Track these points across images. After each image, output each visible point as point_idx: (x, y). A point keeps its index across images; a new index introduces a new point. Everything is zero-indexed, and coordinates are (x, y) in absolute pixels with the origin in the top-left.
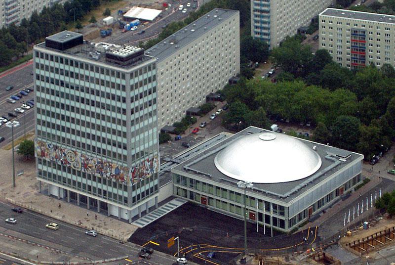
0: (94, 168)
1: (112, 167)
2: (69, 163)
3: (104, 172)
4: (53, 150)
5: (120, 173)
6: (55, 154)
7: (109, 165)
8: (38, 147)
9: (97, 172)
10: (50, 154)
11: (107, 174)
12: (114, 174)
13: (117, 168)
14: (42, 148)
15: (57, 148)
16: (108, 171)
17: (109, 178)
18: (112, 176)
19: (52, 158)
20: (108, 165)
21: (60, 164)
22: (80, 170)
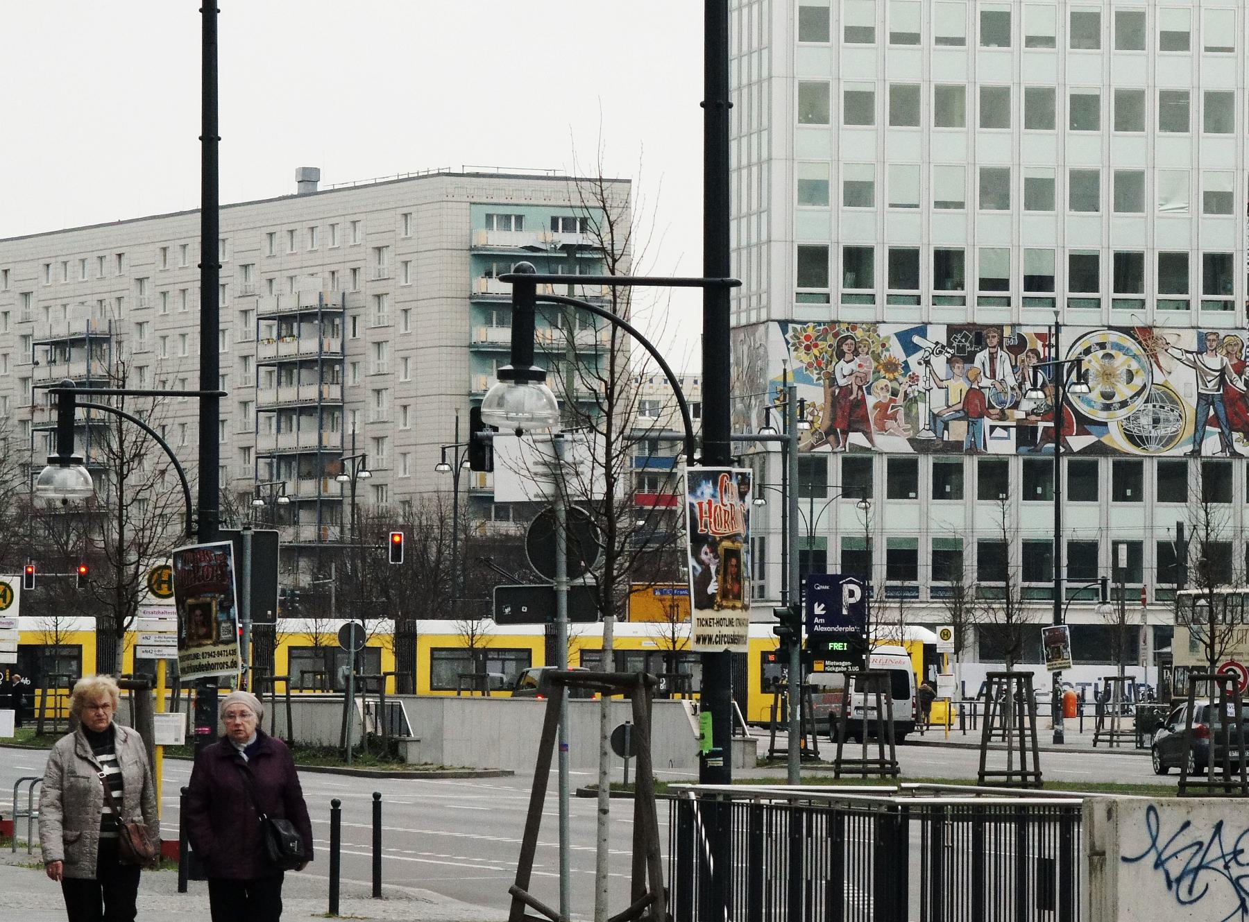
2: (1085, 424)
4: (939, 362)
6: (959, 387)
10: (911, 401)
14: (844, 370)
19: (934, 417)
21: (1002, 445)
22: (1179, 451)
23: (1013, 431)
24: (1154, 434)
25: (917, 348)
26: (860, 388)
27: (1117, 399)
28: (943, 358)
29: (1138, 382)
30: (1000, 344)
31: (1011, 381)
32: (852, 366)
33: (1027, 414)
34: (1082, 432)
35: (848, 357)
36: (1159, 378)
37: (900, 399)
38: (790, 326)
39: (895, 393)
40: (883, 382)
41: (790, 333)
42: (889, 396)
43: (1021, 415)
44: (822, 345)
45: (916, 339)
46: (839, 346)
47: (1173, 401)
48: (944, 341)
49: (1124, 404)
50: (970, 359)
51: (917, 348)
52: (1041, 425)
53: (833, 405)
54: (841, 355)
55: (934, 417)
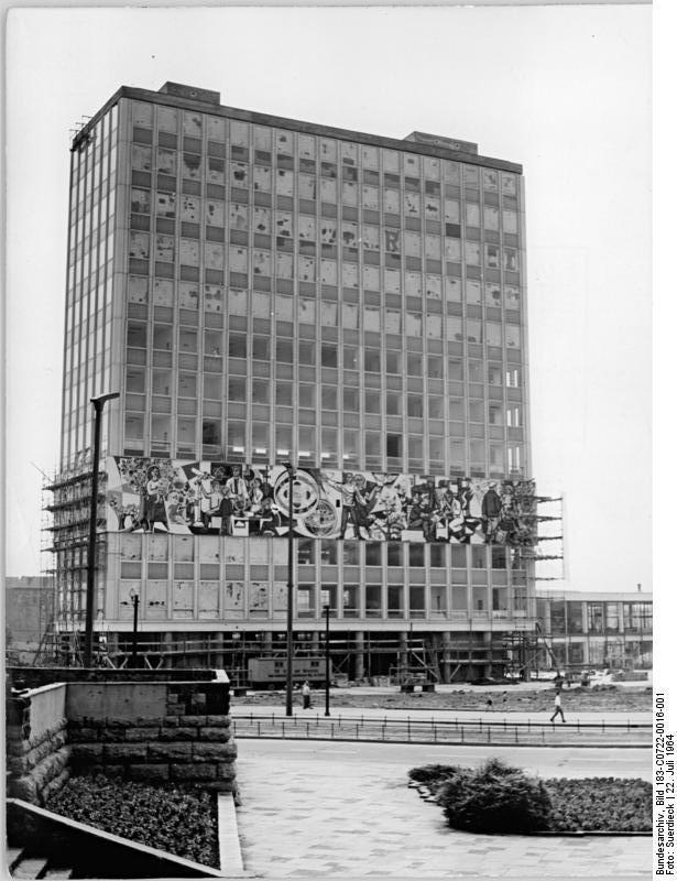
0: (399, 512)
1: (469, 498)
3: (438, 518)
4: (207, 484)
5: (502, 506)
6: (217, 498)
7: (461, 489)
8: (125, 488)
9: (410, 528)
10: (190, 505)
11: (452, 525)
12: (480, 515)
13: (492, 492)
14: (151, 485)
15: (229, 472)
16: (457, 512)
17: (457, 536)
18: (473, 526)
19: (203, 514)
20: (454, 489)
23: (247, 523)
24: (321, 526)
25: (194, 475)
26: (161, 496)
27: (302, 507)
28: (209, 481)
29: (312, 498)
30: (241, 474)
31: (246, 496)
32: (154, 485)
33: (255, 514)
34: (283, 525)
35: (155, 478)
36: (323, 496)
37: (184, 504)
38: (121, 460)
39: (181, 500)
40: (174, 494)
41: (121, 463)
42: (178, 502)
43: (250, 514)
44: (139, 471)
45: (194, 470)
46: (150, 473)
47: (330, 509)
48: (209, 472)
49: (305, 510)
50: (223, 482)
51: (194, 475)
52: (262, 521)
53: (145, 505)
54: (150, 478)
55: (203, 514)
